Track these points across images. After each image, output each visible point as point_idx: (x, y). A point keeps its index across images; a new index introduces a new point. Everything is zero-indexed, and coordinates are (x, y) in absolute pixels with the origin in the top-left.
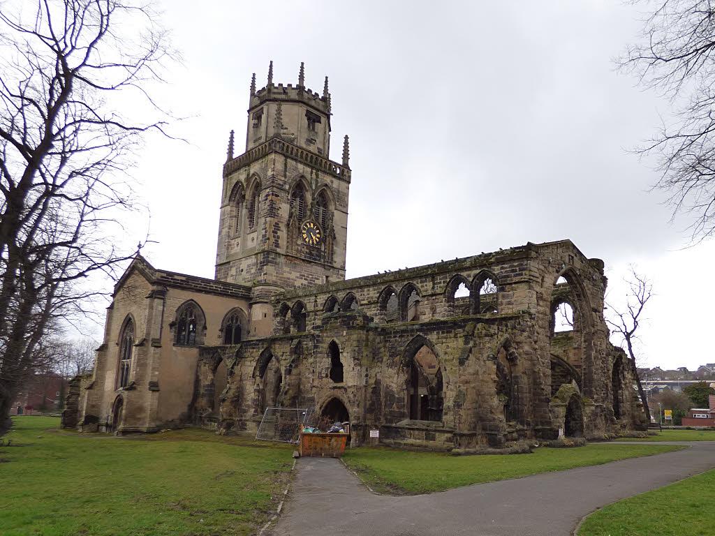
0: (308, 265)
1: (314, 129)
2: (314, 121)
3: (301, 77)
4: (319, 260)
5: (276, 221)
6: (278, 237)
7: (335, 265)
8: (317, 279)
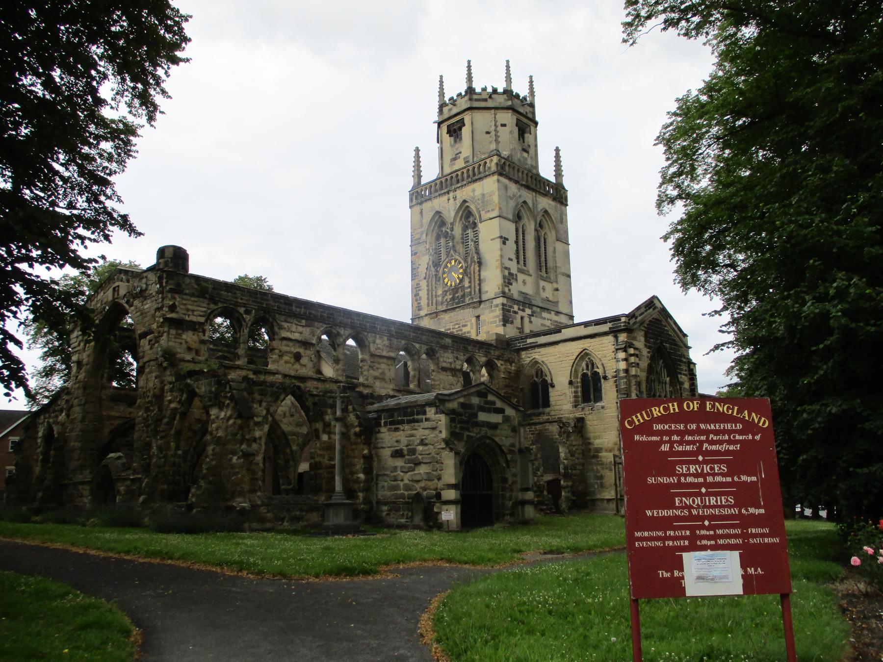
0: (452, 314)
1: (461, 139)
2: (460, 129)
3: (442, 94)
4: (463, 302)
5: (416, 281)
6: (420, 299)
7: (484, 297)
8: (465, 326)
